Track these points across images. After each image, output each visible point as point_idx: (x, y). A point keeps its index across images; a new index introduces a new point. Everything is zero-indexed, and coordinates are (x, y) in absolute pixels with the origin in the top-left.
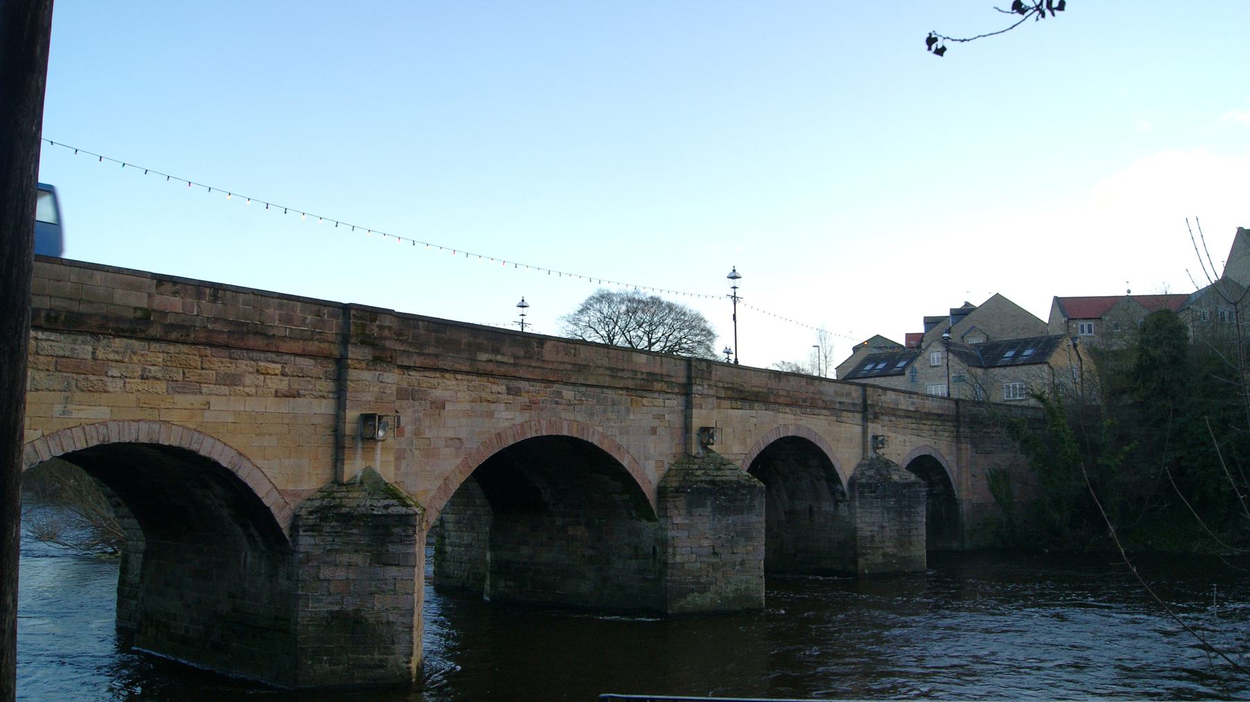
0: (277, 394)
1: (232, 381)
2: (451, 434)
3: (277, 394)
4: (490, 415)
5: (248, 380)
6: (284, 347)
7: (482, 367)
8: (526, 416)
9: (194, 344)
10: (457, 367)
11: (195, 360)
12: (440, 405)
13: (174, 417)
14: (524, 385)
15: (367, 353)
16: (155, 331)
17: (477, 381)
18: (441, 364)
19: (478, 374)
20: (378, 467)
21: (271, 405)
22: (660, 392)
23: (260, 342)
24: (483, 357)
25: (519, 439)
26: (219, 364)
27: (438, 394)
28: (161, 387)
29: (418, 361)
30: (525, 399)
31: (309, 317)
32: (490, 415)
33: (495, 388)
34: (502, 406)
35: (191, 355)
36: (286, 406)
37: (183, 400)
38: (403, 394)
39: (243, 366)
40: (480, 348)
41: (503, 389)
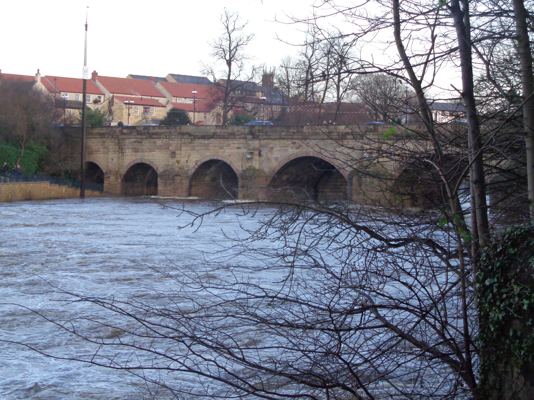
0: (238, 148)
1: (228, 145)
2: (275, 156)
3: (238, 148)
4: (286, 150)
5: (232, 145)
6: (237, 137)
7: (283, 137)
8: (298, 150)
9: (222, 138)
10: (276, 137)
11: (223, 142)
12: (272, 148)
13: (220, 154)
14: (297, 141)
15: (251, 137)
16: (215, 137)
17: (282, 141)
18: (271, 137)
19: (283, 139)
20: (254, 164)
21: (235, 151)
22: (349, 139)
23: (232, 136)
24: (283, 134)
25: (296, 157)
26: (226, 142)
27: (271, 145)
28: (217, 148)
29: (265, 137)
30: (297, 145)
31: (243, 130)
32: (286, 150)
33: (288, 143)
34: (290, 148)
35: (222, 141)
36: (238, 151)
37: (221, 150)
38: (261, 146)
39: (230, 142)
40: (283, 132)
41: (290, 142)
